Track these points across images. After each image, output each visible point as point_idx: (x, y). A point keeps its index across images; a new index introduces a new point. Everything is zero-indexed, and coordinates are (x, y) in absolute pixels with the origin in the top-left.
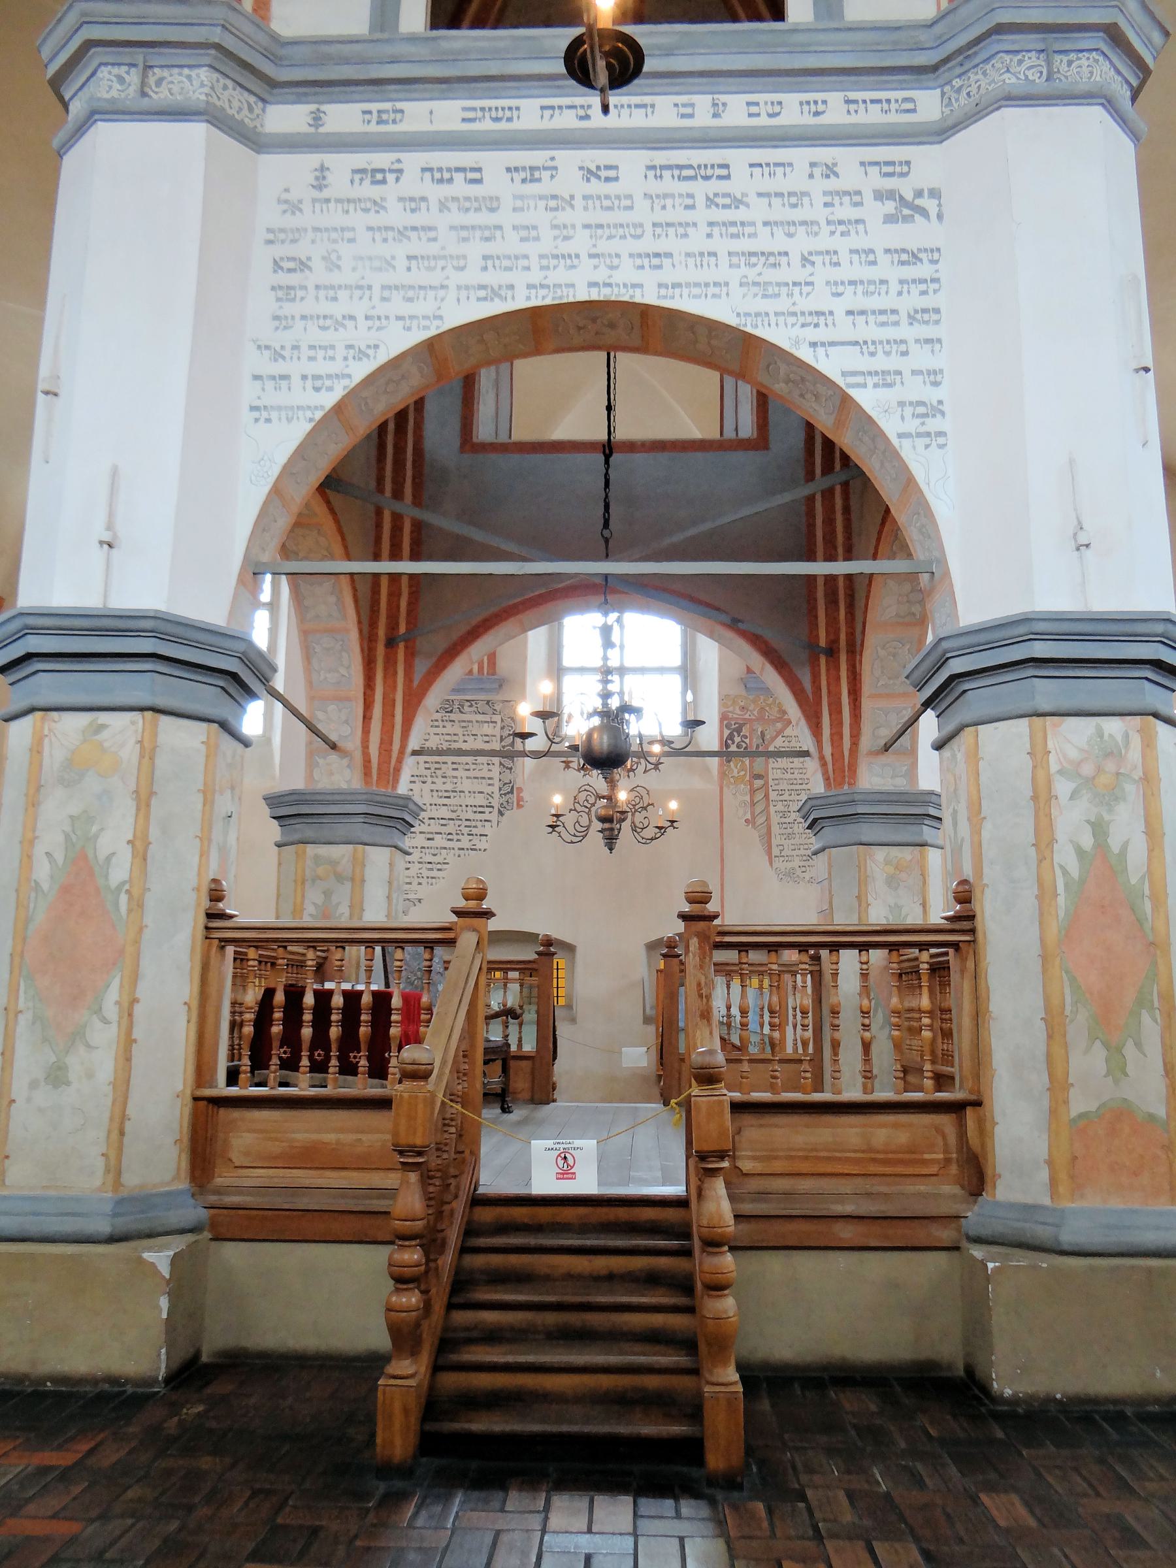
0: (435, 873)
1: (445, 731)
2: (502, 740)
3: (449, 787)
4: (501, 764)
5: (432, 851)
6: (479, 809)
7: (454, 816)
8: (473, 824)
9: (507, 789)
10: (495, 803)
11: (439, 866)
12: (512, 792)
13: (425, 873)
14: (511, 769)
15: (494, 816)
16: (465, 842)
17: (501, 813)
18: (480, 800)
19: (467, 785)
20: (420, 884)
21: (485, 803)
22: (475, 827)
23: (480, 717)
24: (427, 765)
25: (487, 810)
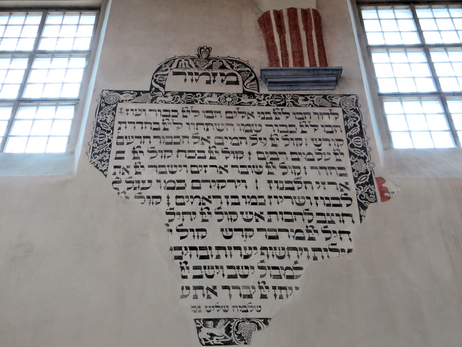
0: (284, 282)
1: (278, 122)
2: (347, 130)
3: (291, 177)
4: (351, 153)
5: (278, 253)
6: (333, 202)
7: (301, 209)
8: (328, 218)
9: (364, 179)
10: (353, 193)
11: (289, 273)
12: (371, 182)
13: (271, 282)
14: (364, 158)
15: (354, 209)
16: (321, 241)
17: (362, 206)
18: (332, 192)
19: (313, 176)
20: (263, 297)
21: (339, 194)
22: (332, 222)
23: (318, 110)
24: (261, 156)
25: (344, 203)
